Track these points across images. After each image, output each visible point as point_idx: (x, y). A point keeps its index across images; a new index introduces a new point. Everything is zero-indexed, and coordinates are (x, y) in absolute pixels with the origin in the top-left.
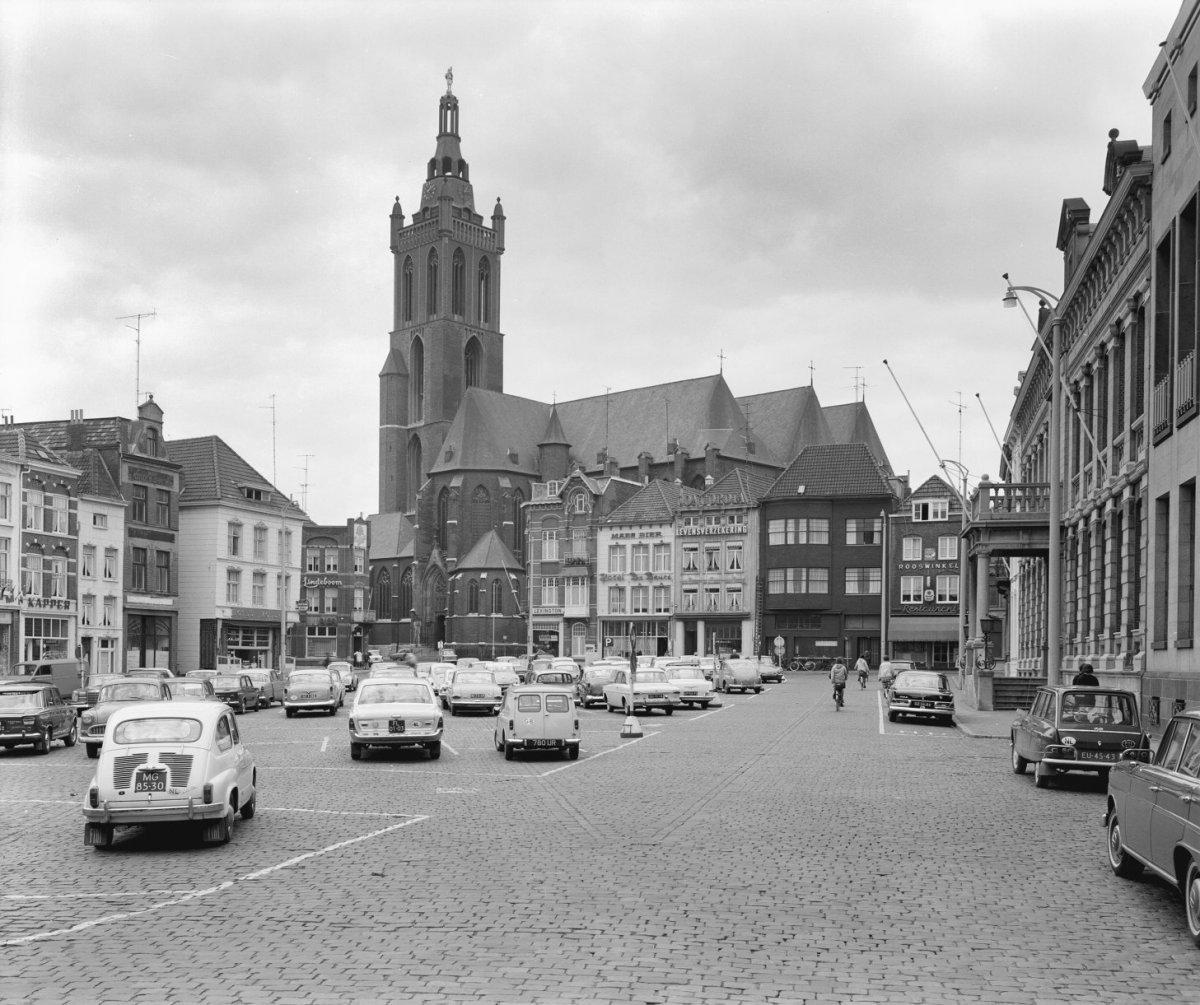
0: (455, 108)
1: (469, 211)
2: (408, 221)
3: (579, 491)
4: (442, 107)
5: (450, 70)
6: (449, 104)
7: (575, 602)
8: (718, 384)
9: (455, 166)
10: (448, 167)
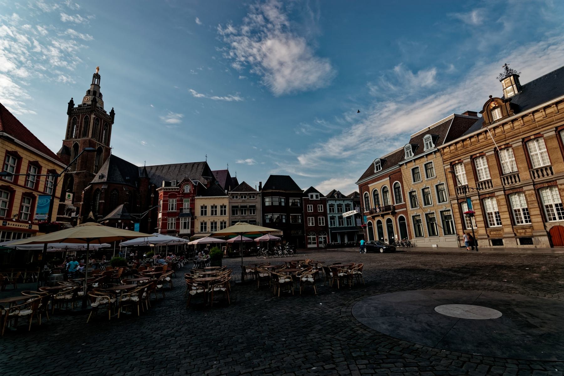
1: (102, 108)
2: (76, 106)
3: (187, 184)
4: (94, 77)
6: (97, 76)
7: (185, 228)
8: (205, 165)
9: (97, 95)
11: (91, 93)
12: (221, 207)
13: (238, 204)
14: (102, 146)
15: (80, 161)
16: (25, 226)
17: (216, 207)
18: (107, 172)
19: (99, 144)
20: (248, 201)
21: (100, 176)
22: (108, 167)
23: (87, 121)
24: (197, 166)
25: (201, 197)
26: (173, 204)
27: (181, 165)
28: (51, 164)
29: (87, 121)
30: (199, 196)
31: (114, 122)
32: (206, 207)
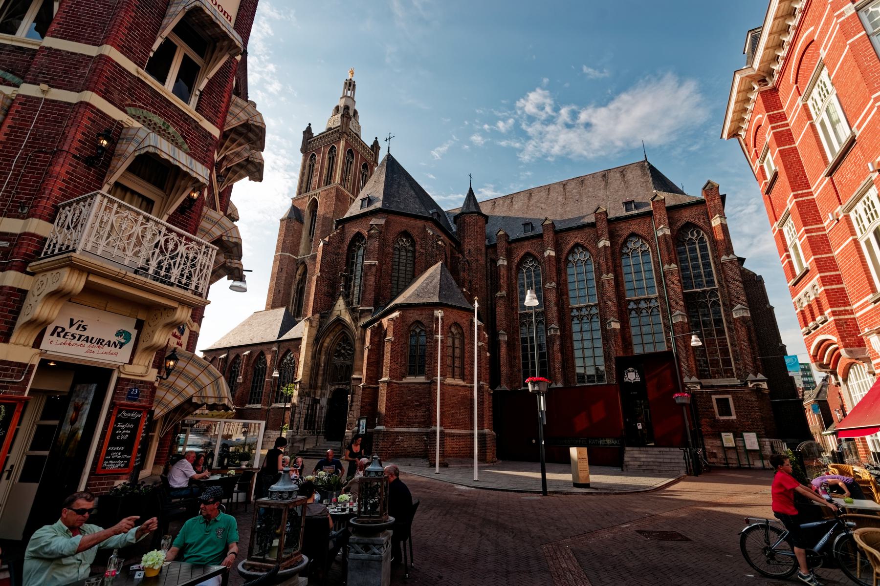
0: (354, 85)
5: (352, 71)
6: (350, 85)
10: (347, 113)
11: (341, 111)
15: (319, 232)
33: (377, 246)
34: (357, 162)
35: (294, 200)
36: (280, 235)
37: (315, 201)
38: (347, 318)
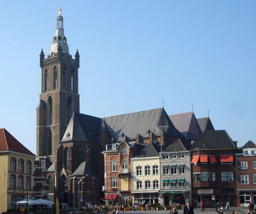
0: (62, 20)
1: (67, 54)
2: (46, 57)
9: (62, 39)
10: (61, 39)
12: (154, 167)
13: (169, 164)
14: (71, 95)
16: (21, 192)
17: (149, 167)
18: (72, 130)
19: (69, 93)
20: (177, 161)
21: (67, 135)
22: (72, 126)
23: (56, 72)
24: (154, 113)
25: (136, 158)
26: (114, 165)
27: (139, 113)
28: (28, 158)
29: (56, 72)
30: (134, 158)
31: (80, 66)
32: (140, 168)
33: (71, 154)
34: (68, 71)
35: (41, 95)
36: (37, 117)
37: (50, 96)
38: (65, 174)
